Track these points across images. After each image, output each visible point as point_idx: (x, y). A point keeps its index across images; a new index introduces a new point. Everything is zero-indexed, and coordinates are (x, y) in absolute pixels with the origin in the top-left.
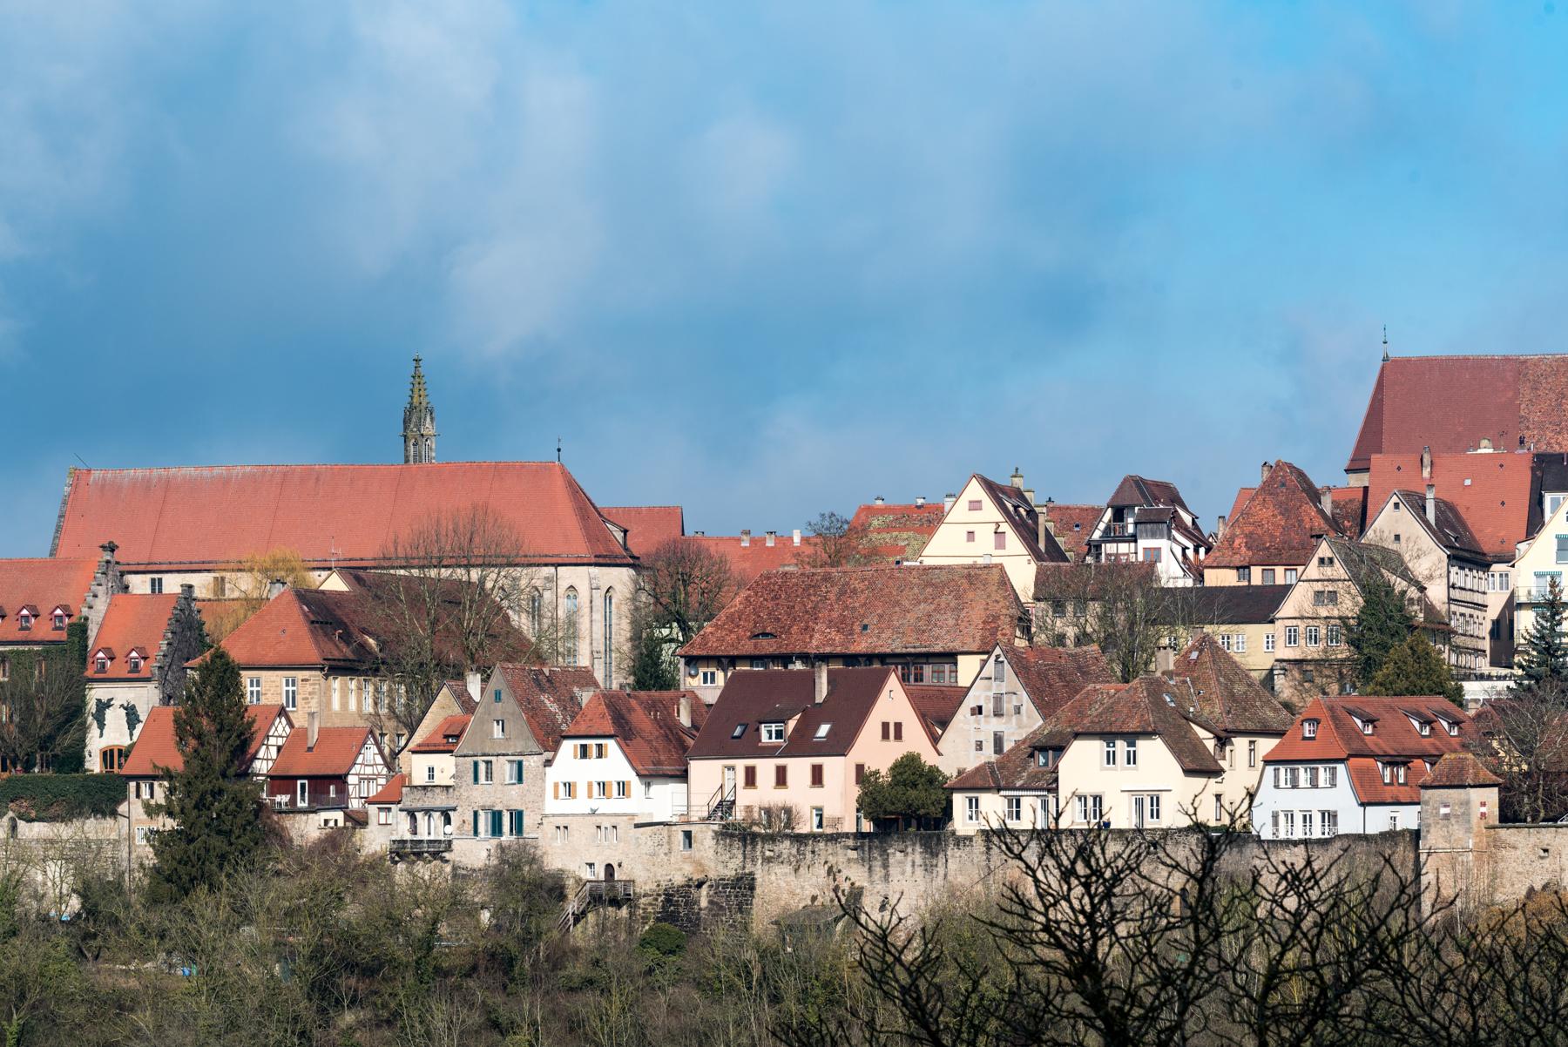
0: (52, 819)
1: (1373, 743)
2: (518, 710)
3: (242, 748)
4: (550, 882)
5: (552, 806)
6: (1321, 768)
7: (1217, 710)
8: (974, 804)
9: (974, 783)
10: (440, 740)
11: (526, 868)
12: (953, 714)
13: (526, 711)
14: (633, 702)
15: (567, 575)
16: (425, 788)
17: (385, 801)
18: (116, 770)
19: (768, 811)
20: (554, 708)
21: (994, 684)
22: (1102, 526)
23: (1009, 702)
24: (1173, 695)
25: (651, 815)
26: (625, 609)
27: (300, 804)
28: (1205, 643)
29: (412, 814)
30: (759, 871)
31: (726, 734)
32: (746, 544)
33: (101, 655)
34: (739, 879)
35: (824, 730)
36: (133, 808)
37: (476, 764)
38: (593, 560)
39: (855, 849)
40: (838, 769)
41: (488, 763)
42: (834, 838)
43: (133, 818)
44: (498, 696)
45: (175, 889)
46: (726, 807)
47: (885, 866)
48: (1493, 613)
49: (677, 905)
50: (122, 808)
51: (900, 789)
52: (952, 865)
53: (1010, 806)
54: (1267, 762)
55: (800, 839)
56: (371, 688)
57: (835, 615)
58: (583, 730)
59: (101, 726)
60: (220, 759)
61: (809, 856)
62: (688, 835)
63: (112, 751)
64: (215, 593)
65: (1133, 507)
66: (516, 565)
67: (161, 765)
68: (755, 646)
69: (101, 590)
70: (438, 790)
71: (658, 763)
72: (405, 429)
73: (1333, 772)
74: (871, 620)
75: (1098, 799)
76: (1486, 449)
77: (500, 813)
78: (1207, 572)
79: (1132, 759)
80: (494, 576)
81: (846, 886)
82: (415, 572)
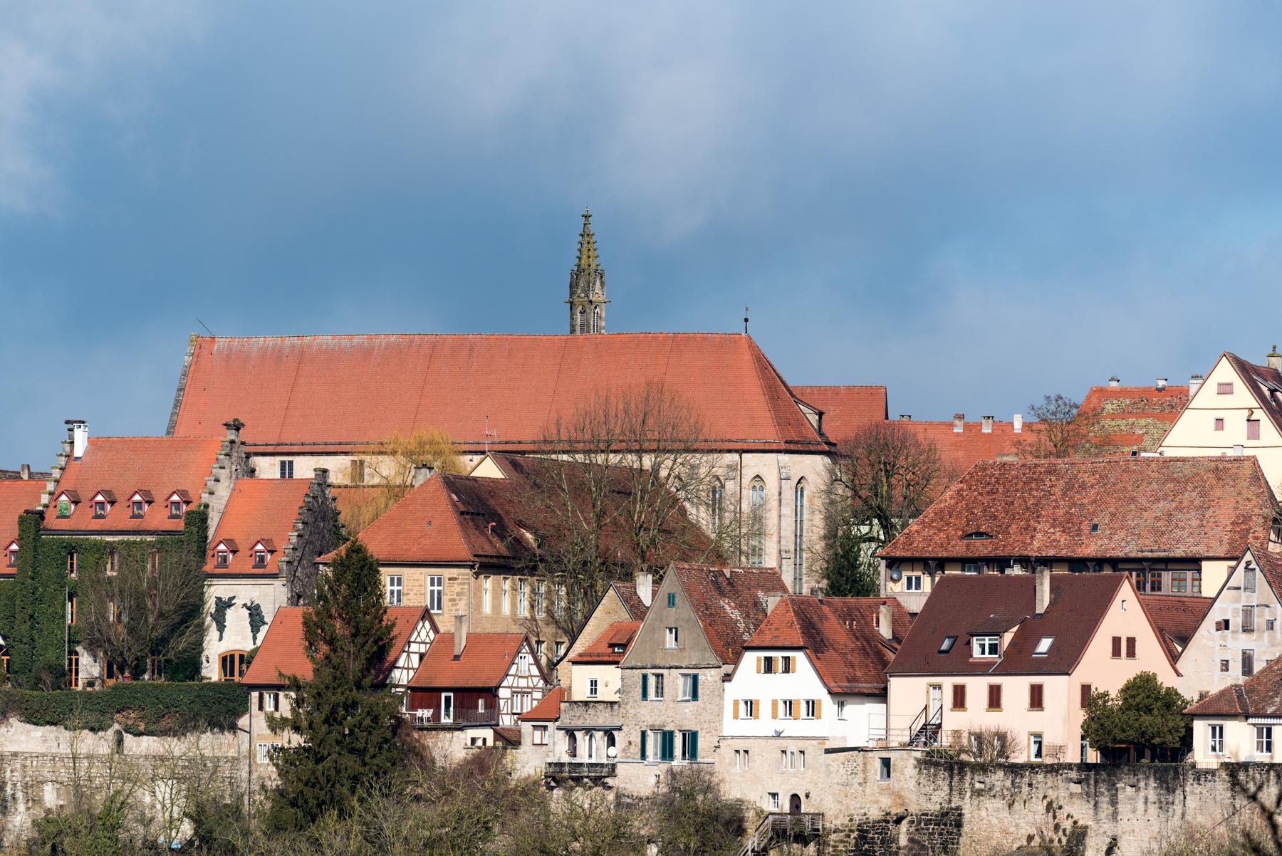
0: (164, 733)
2: (693, 615)
3: (380, 655)
4: (727, 815)
5: (730, 726)
8: (1217, 732)
9: (1221, 708)
11: (700, 798)
12: (1196, 629)
13: (704, 617)
14: (826, 609)
16: (586, 703)
17: (540, 719)
18: (237, 678)
19: (979, 737)
20: (735, 614)
21: (1243, 594)
23: (1261, 615)
25: (844, 738)
26: (818, 502)
27: (445, 720)
29: (571, 733)
30: (967, 806)
31: (932, 648)
32: (958, 430)
33: (222, 547)
34: (945, 814)
35: (1045, 645)
36: (255, 721)
37: (645, 677)
38: (783, 446)
39: (1079, 782)
40: (1061, 691)
41: (658, 676)
42: (1054, 769)
43: (254, 734)
44: (671, 600)
45: (300, 814)
46: (930, 731)
47: (1114, 802)
49: (872, 842)
50: (243, 722)
51: (1132, 714)
52: (1192, 803)
53: (1260, 735)
55: (1016, 770)
56: (527, 589)
57: (1060, 512)
59: (221, 627)
60: (354, 667)
61: (1025, 789)
62: (886, 763)
63: (232, 656)
64: (353, 479)
66: (695, 451)
67: (287, 672)
68: (968, 546)
70: (601, 707)
71: (854, 679)
72: (572, 294)
74: (1102, 519)
77: (671, 733)
80: (669, 463)
81: (1067, 825)
82: (580, 458)
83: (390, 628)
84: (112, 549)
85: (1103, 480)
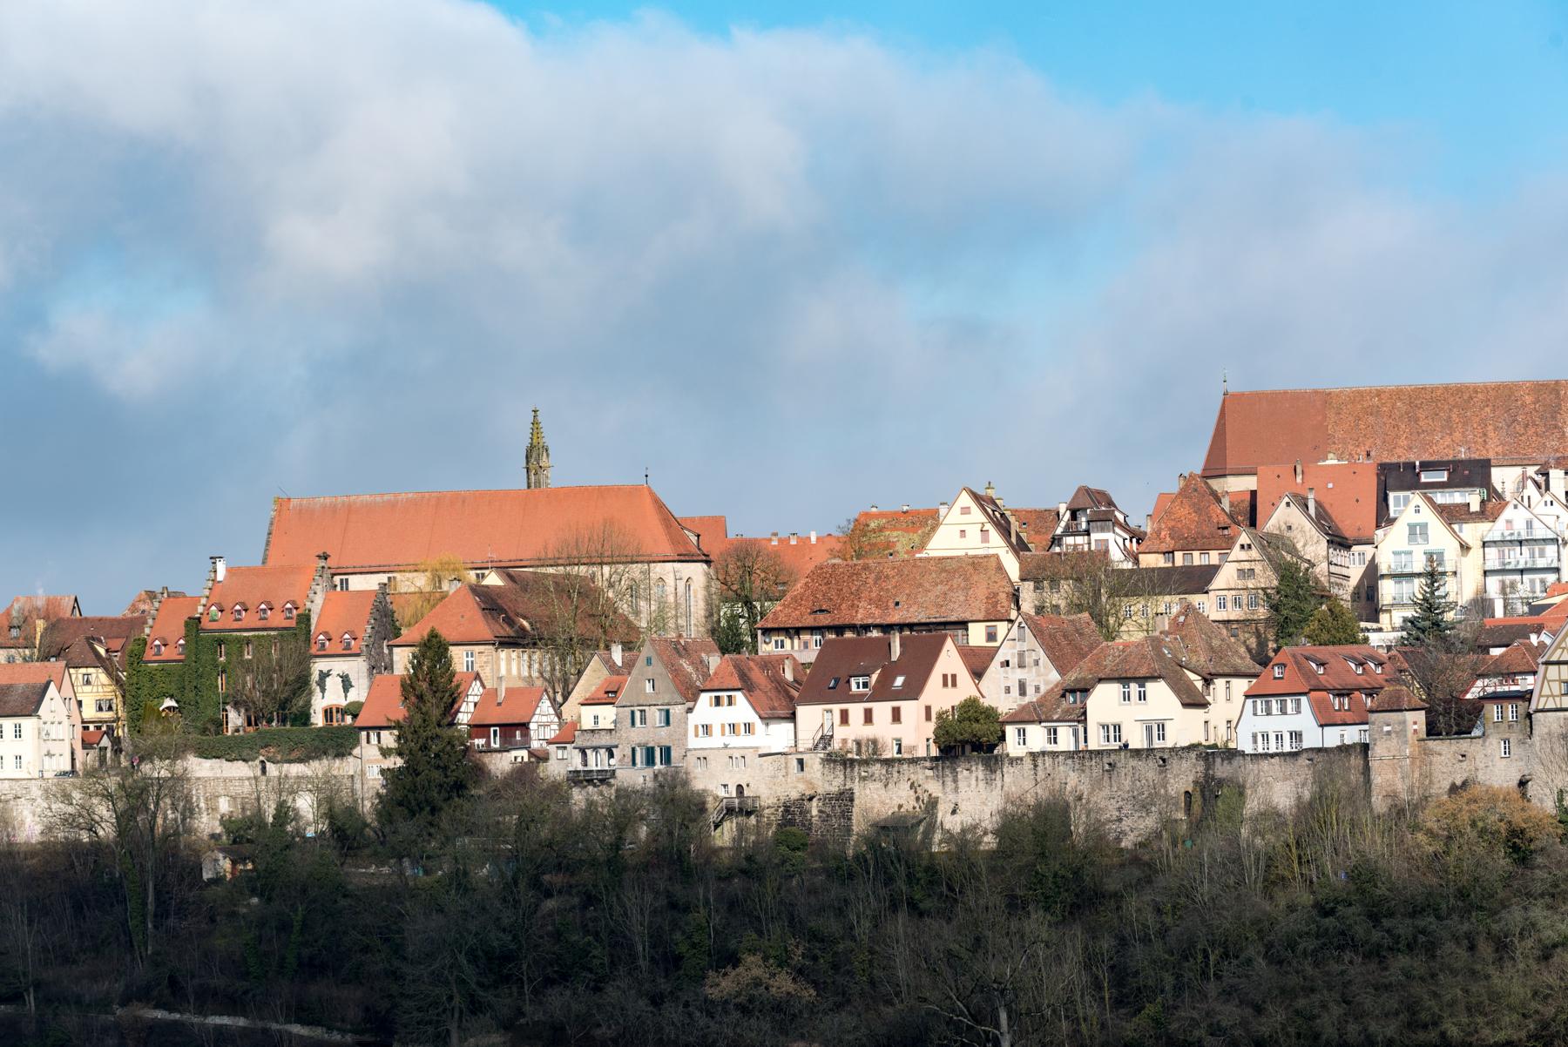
1: (1327, 681)
3: (451, 705)
8: (1022, 733)
9: (1022, 718)
10: (602, 695)
15: (658, 569)
16: (593, 731)
20: (690, 669)
22: (1063, 524)
24: (1169, 649)
28: (1188, 610)
29: (583, 751)
30: (857, 788)
31: (826, 684)
32: (775, 543)
35: (899, 681)
42: (914, 761)
46: (826, 740)
47: (955, 781)
48: (1354, 582)
50: (356, 751)
52: (1007, 779)
54: (1247, 696)
55: (888, 762)
56: (526, 657)
59: (323, 690)
60: (436, 713)
62: (801, 762)
69: (318, 589)
71: (774, 708)
73: (1298, 703)
75: (1118, 728)
83: (458, 686)
84: (248, 641)
85: (900, 573)
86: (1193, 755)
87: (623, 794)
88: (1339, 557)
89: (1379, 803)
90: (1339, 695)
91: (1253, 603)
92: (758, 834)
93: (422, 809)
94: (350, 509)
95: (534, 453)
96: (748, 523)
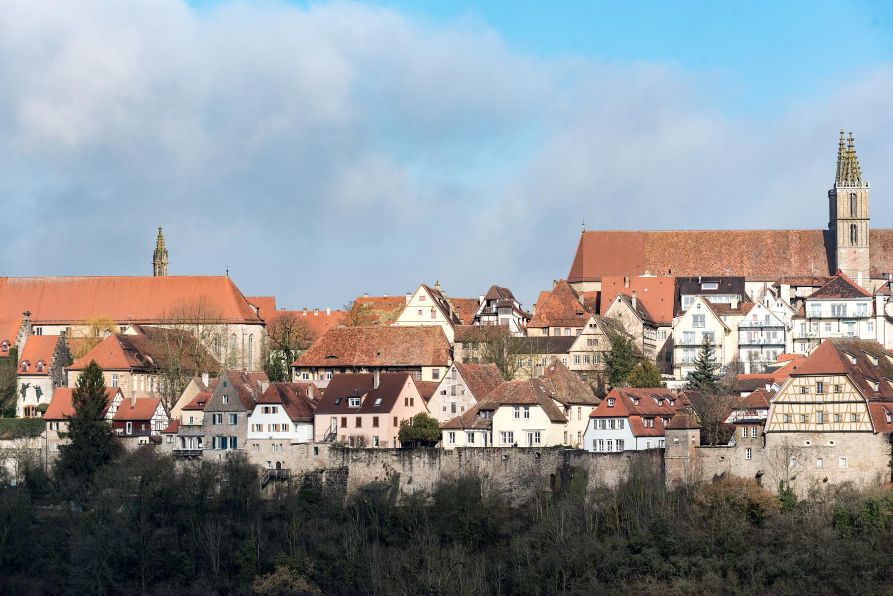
1: (639, 409)
5: (251, 435)
6: (616, 420)
7: (564, 394)
8: (453, 436)
9: (453, 426)
10: (195, 404)
15: (233, 328)
16: (189, 426)
17: (170, 432)
19: (352, 439)
20: (250, 390)
22: (481, 308)
24: (544, 387)
28: (556, 363)
29: (183, 439)
31: (333, 402)
32: (305, 314)
34: (341, 469)
35: (378, 401)
40: (384, 418)
42: (386, 451)
46: (333, 436)
47: (411, 463)
48: (658, 349)
49: (311, 481)
50: (44, 434)
51: (419, 428)
54: (591, 417)
55: (370, 451)
56: (149, 379)
57: (364, 348)
58: (266, 400)
59: (24, 396)
60: (93, 412)
61: (374, 459)
65: (495, 300)
69: (23, 333)
71: (301, 416)
73: (622, 422)
74: (381, 351)
75: (511, 434)
76: (647, 275)
77: (226, 438)
78: (529, 330)
79: (527, 415)
83: (107, 396)
85: (381, 335)
86: (557, 452)
87: (207, 465)
88: (650, 334)
89: (670, 485)
90: (647, 418)
91: (596, 360)
92: (289, 492)
93: (82, 471)
94: (44, 285)
95: (159, 255)
96: (290, 302)
